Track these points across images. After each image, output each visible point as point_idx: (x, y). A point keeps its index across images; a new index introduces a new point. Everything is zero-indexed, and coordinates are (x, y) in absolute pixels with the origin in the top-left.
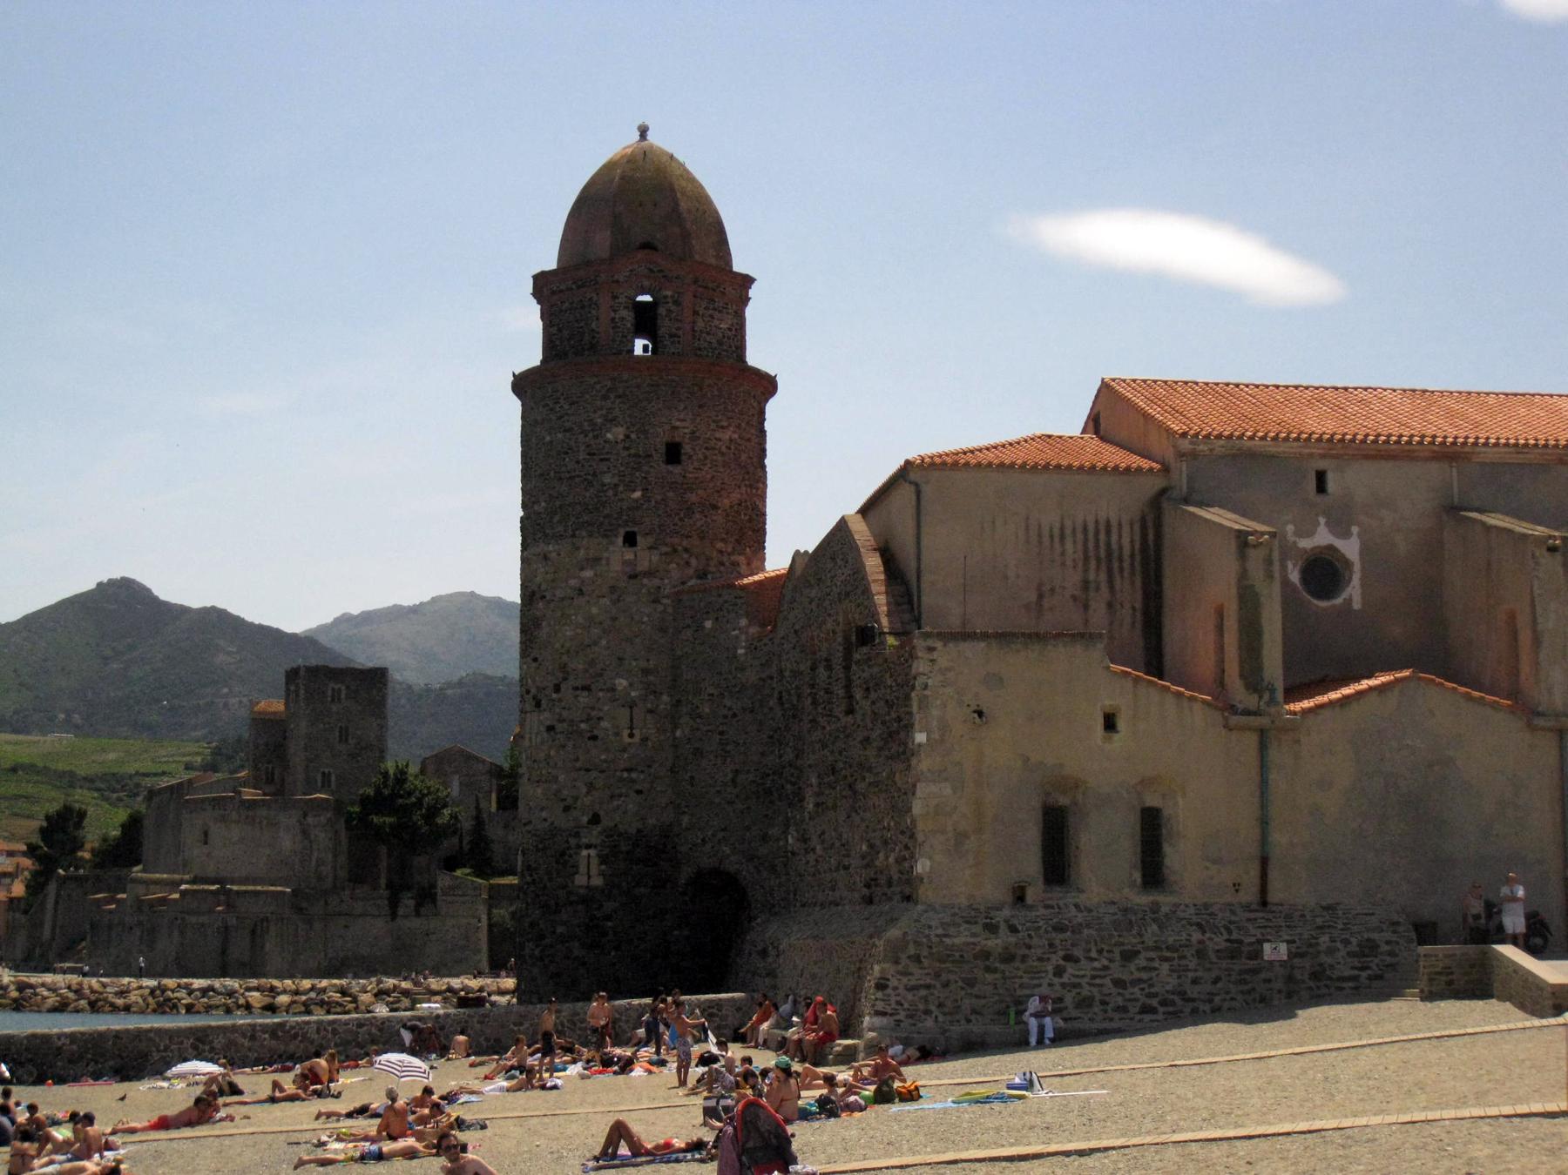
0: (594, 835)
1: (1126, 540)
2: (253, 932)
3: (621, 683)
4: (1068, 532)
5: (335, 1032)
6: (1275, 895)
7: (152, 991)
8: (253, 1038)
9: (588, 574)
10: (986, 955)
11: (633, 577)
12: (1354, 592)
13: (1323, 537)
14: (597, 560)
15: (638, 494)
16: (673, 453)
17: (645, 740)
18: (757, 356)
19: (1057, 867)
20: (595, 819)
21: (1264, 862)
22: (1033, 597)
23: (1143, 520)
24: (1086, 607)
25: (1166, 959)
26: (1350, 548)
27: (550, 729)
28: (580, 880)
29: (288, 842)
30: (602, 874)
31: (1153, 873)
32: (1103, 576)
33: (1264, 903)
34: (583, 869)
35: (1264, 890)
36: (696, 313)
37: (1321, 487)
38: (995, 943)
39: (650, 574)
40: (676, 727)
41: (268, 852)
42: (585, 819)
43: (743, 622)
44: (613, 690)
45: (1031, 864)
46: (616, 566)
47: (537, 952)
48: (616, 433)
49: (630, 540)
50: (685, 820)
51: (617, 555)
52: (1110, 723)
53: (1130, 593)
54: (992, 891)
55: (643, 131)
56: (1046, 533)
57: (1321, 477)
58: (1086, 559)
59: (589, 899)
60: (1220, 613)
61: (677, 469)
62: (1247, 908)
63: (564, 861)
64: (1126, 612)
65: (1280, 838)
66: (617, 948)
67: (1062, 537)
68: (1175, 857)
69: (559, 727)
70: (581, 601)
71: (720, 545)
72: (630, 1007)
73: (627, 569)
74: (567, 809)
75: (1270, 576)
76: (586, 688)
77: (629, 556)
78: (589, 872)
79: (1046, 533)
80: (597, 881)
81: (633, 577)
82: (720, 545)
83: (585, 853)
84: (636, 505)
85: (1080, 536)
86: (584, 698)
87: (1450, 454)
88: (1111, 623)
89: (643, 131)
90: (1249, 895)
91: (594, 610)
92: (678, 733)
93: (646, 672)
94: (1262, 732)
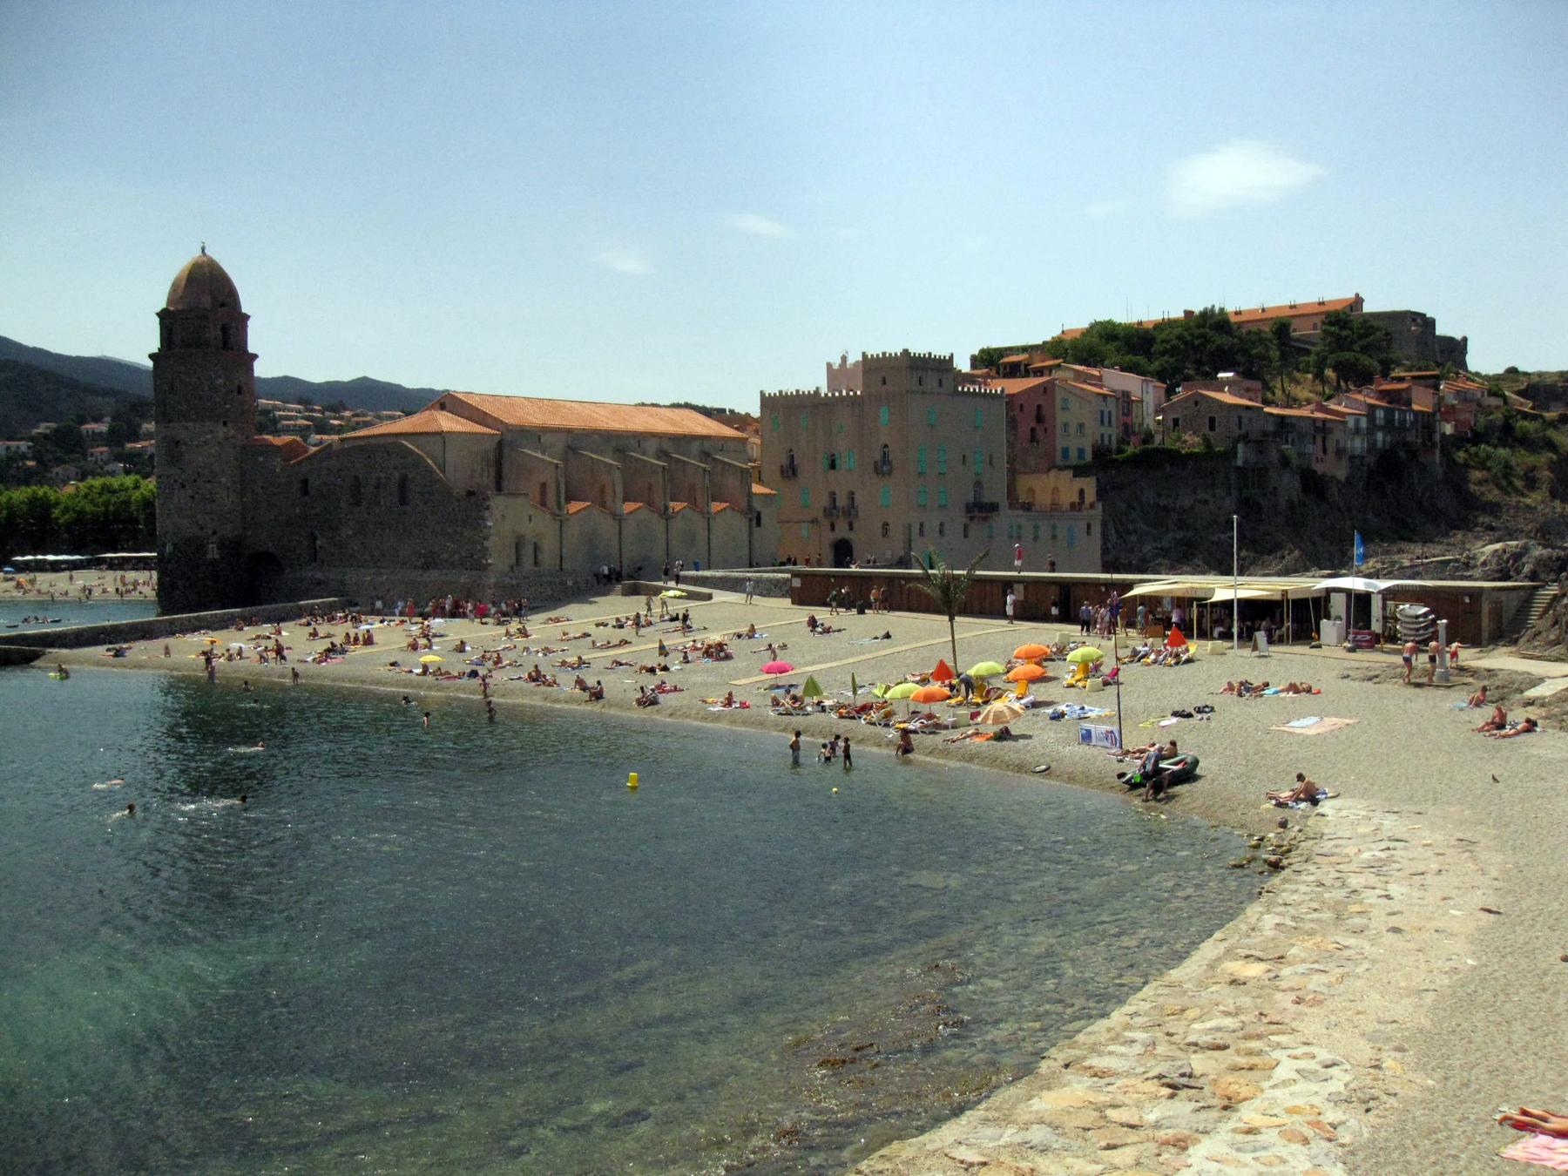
0: (214, 538)
1: (492, 456)
8: (190, 621)
9: (209, 436)
10: (513, 586)
14: (212, 432)
15: (228, 406)
18: (251, 349)
20: (215, 533)
21: (561, 557)
22: (469, 473)
27: (192, 497)
28: (209, 556)
30: (220, 554)
33: (562, 569)
34: (210, 552)
35: (561, 565)
38: (514, 582)
39: (233, 437)
40: (243, 496)
42: (210, 532)
43: (279, 460)
44: (220, 482)
46: (221, 435)
47: (187, 584)
48: (220, 381)
50: (250, 533)
51: (221, 431)
52: (530, 517)
53: (493, 473)
54: (506, 568)
55: (203, 249)
59: (213, 562)
60: (543, 486)
63: (201, 547)
64: (491, 478)
69: (197, 496)
70: (206, 447)
72: (308, 604)
74: (202, 528)
76: (209, 481)
77: (225, 430)
78: (213, 552)
80: (217, 557)
81: (227, 439)
83: (211, 546)
86: (209, 486)
87: (569, 431)
89: (203, 249)
90: (558, 568)
91: (213, 451)
92: (245, 500)
94: (561, 522)
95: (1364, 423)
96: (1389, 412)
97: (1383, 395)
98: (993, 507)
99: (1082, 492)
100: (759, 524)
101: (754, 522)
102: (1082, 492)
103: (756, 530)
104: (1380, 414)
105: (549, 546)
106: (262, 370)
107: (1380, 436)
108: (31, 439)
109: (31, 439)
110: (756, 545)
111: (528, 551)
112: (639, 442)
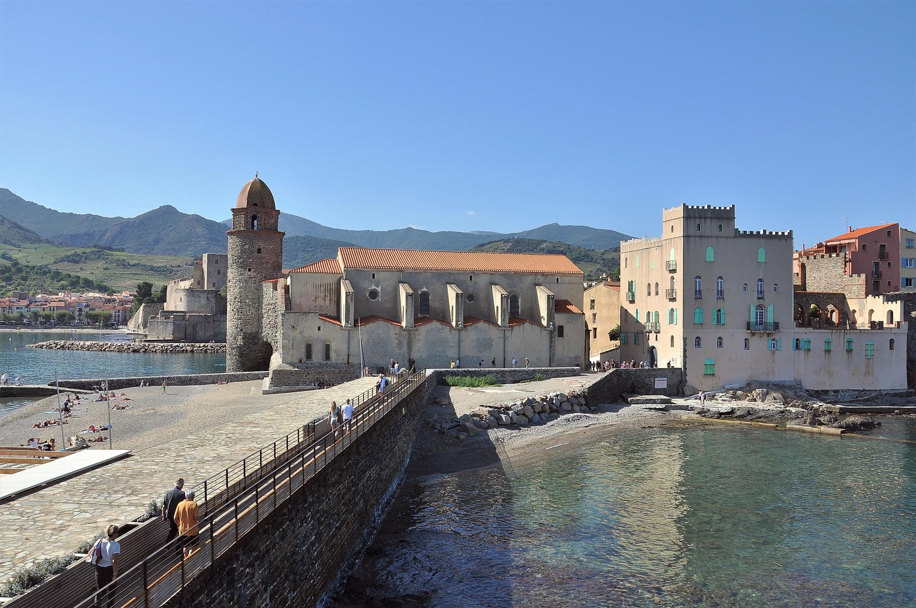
2: (193, 328)
3: (247, 301)
4: (322, 285)
5: (180, 379)
6: (350, 362)
7: (162, 347)
11: (250, 278)
12: (379, 299)
13: (373, 287)
14: (243, 274)
16: (259, 251)
17: (252, 313)
19: (309, 355)
20: (242, 330)
21: (348, 355)
22: (314, 298)
23: (337, 283)
24: (325, 301)
25: (326, 374)
26: (379, 289)
28: (238, 343)
29: (203, 302)
31: (328, 357)
32: (329, 294)
33: (348, 363)
36: (265, 219)
37: (374, 277)
41: (198, 304)
44: (245, 302)
45: (303, 355)
48: (247, 247)
49: (250, 270)
52: (319, 328)
53: (334, 298)
55: (257, 176)
56: (317, 285)
57: (374, 275)
58: (325, 291)
61: (260, 255)
62: (344, 363)
65: (351, 350)
66: (246, 357)
67: (321, 287)
68: (333, 355)
71: (270, 271)
73: (249, 277)
75: (352, 301)
77: (249, 273)
79: (317, 285)
81: (250, 278)
82: (270, 271)
84: (251, 262)
85: (324, 287)
86: (239, 304)
87: (400, 270)
88: (330, 304)
90: (346, 361)
93: (253, 299)
101: (556, 333)
103: (558, 341)
112: (471, 277)
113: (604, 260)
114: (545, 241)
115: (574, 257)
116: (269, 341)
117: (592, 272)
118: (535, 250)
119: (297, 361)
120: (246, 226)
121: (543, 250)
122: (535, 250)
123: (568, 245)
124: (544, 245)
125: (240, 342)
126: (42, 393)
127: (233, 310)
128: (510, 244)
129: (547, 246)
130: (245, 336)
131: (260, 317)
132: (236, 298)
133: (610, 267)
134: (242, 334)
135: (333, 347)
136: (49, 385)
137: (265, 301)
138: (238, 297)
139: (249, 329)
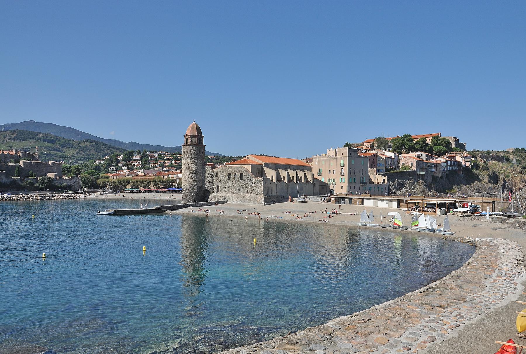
20: (196, 185)
48: (198, 151)
49: (199, 161)
87: (276, 164)
95: (445, 164)
96: (451, 161)
97: (449, 157)
98: (366, 183)
99: (384, 180)
100: (315, 186)
102: (384, 180)
104: (449, 162)
105: (274, 189)
106: (206, 149)
107: (449, 167)
108: (104, 160)
109: (104, 160)
110: (314, 190)
111: (270, 190)
113: (80, 146)
114: (40, 133)
115: (61, 144)
116: (209, 189)
117: (73, 154)
118: (34, 138)
119: (266, 194)
120: (197, 143)
121: (40, 138)
122: (34, 138)
123: (56, 136)
124: (40, 136)
125: (196, 190)
126: (159, 211)
127: (191, 177)
128: (16, 134)
129: (42, 136)
130: (198, 188)
131: (203, 181)
132: (193, 172)
133: (85, 151)
134: (197, 187)
135: (273, 189)
136: (155, 208)
137: (206, 174)
138: (195, 171)
139: (200, 185)
